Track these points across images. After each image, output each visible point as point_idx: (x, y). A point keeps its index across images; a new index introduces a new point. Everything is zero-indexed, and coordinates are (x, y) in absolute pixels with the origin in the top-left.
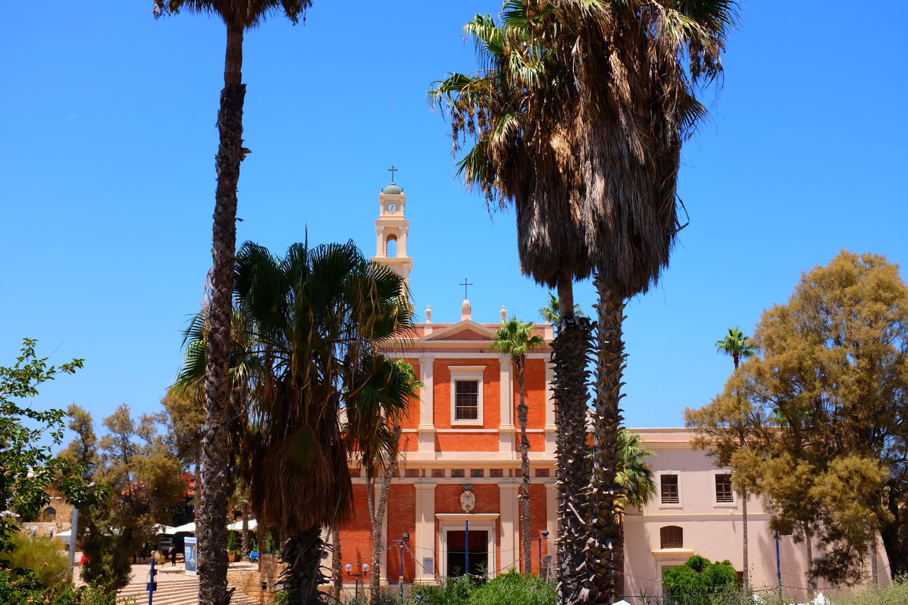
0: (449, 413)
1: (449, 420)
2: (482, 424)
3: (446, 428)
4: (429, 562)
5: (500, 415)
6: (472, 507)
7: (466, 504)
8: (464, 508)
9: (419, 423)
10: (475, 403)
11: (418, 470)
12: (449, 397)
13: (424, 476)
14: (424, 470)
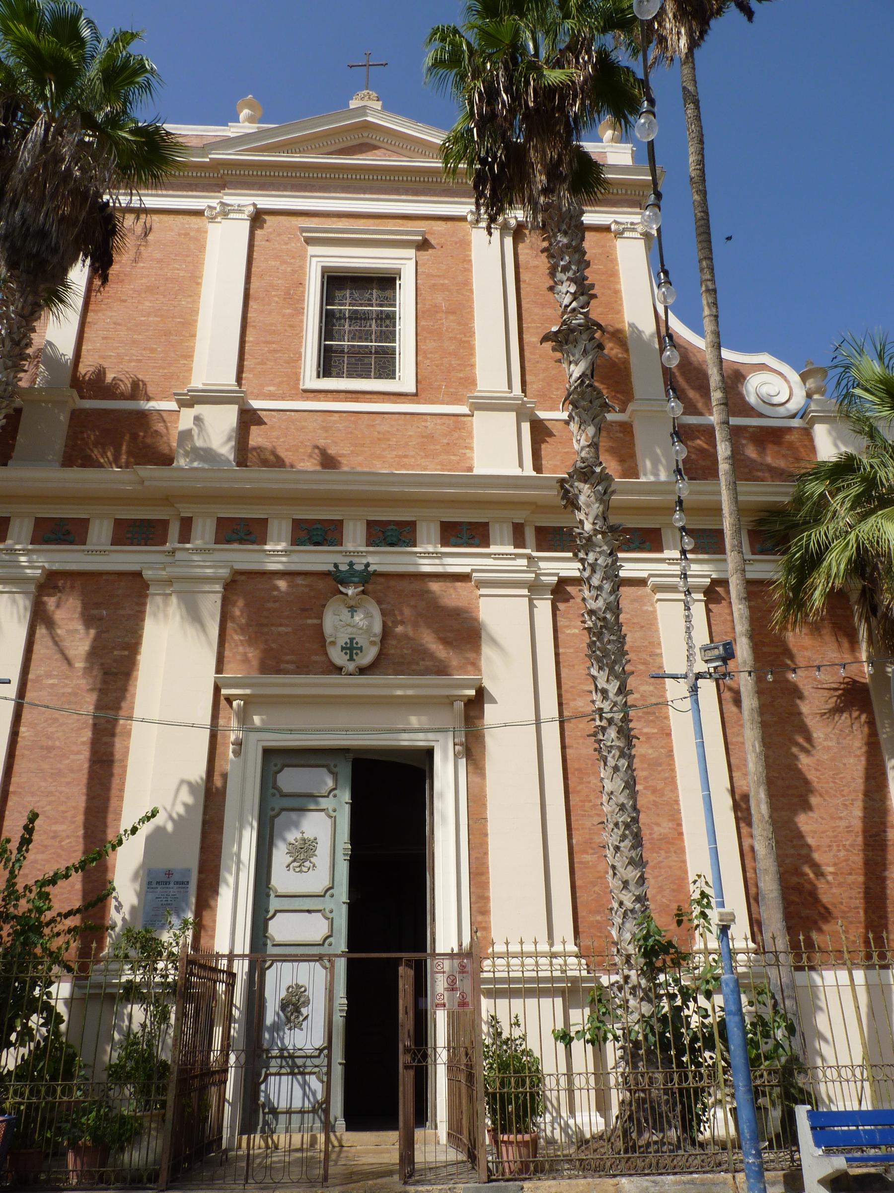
0: (296, 358)
1: (296, 377)
2: (412, 389)
3: (283, 398)
4: (173, 889)
5: (473, 366)
6: (368, 656)
7: (342, 640)
8: (337, 656)
9: (211, 449)
10: (391, 336)
11: (165, 524)
12: (299, 310)
13: (185, 537)
14: (186, 524)
